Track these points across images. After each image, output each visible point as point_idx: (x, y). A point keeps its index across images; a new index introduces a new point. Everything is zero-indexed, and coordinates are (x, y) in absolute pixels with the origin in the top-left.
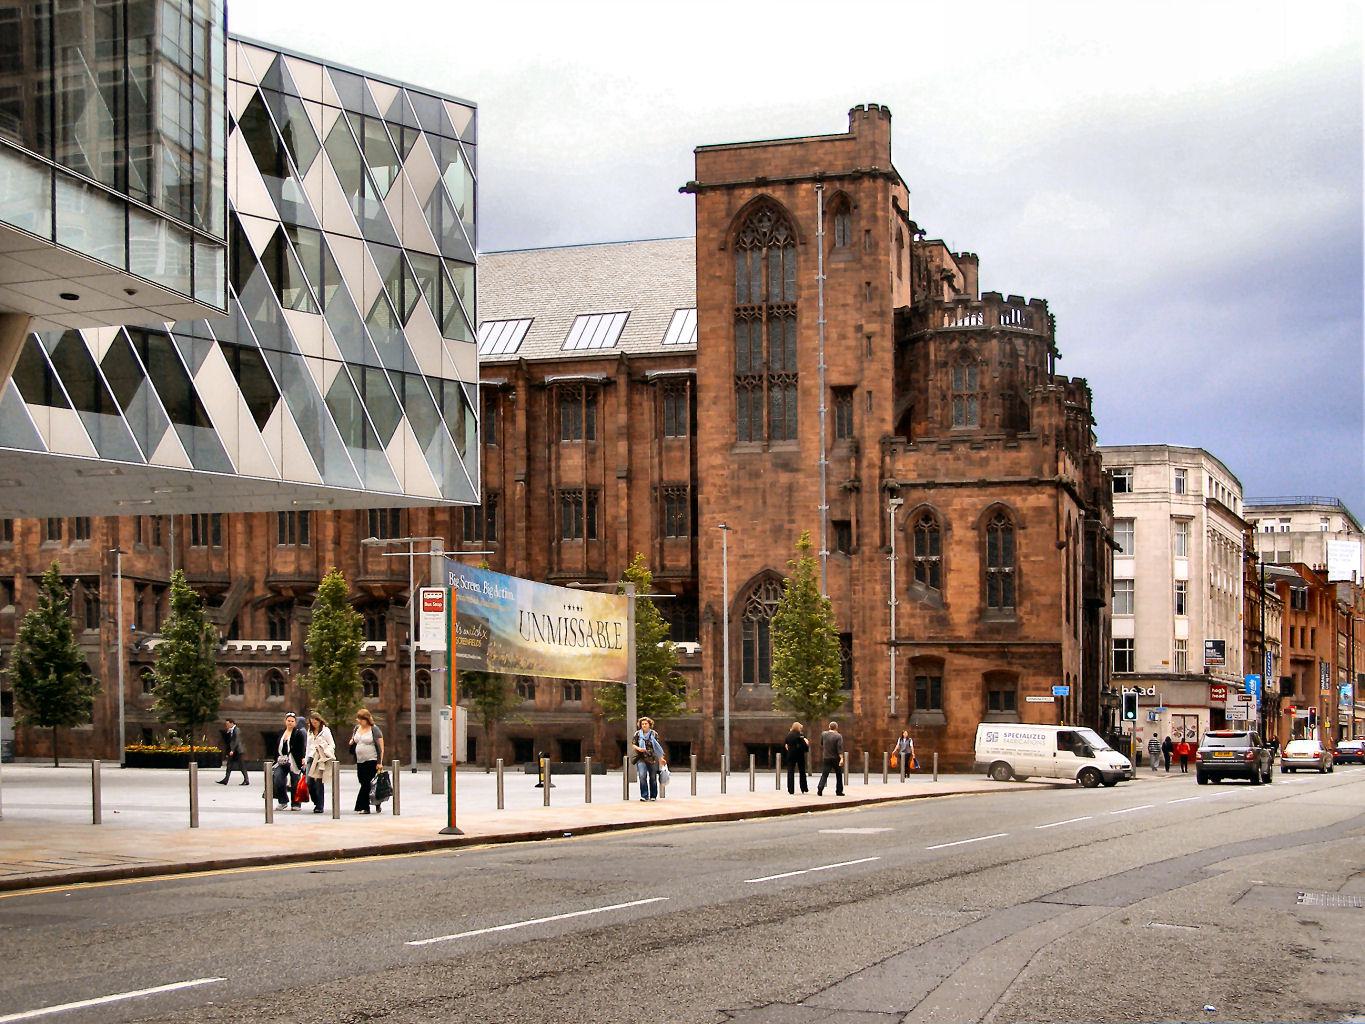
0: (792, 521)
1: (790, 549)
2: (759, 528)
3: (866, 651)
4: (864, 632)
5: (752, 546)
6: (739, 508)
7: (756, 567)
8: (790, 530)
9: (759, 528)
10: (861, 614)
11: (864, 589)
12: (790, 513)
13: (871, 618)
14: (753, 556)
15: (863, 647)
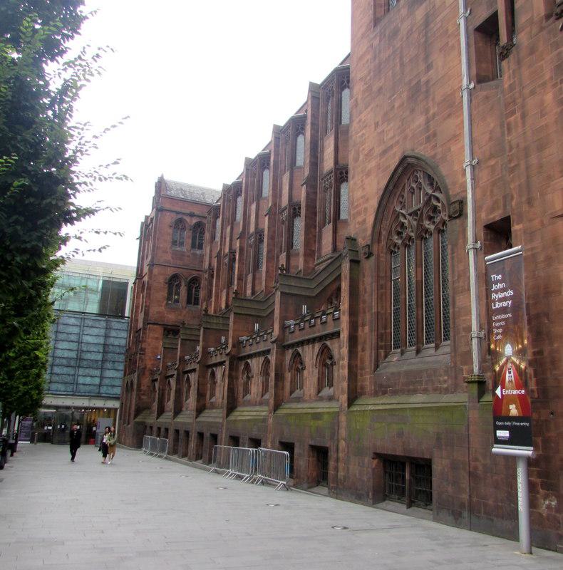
0: (429, 68)
1: (427, 111)
2: (397, 105)
3: (537, 243)
4: (530, 202)
5: (391, 134)
6: (380, 89)
7: (394, 163)
8: (428, 82)
9: (397, 105)
10: (523, 166)
11: (524, 116)
12: (426, 58)
13: (541, 166)
14: (391, 147)
15: (530, 235)
